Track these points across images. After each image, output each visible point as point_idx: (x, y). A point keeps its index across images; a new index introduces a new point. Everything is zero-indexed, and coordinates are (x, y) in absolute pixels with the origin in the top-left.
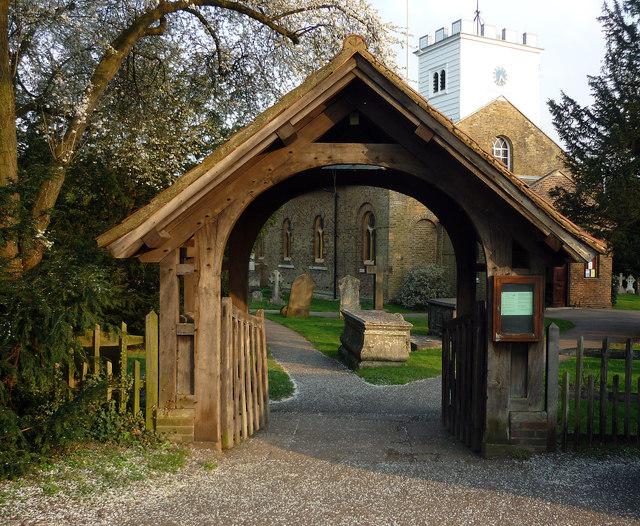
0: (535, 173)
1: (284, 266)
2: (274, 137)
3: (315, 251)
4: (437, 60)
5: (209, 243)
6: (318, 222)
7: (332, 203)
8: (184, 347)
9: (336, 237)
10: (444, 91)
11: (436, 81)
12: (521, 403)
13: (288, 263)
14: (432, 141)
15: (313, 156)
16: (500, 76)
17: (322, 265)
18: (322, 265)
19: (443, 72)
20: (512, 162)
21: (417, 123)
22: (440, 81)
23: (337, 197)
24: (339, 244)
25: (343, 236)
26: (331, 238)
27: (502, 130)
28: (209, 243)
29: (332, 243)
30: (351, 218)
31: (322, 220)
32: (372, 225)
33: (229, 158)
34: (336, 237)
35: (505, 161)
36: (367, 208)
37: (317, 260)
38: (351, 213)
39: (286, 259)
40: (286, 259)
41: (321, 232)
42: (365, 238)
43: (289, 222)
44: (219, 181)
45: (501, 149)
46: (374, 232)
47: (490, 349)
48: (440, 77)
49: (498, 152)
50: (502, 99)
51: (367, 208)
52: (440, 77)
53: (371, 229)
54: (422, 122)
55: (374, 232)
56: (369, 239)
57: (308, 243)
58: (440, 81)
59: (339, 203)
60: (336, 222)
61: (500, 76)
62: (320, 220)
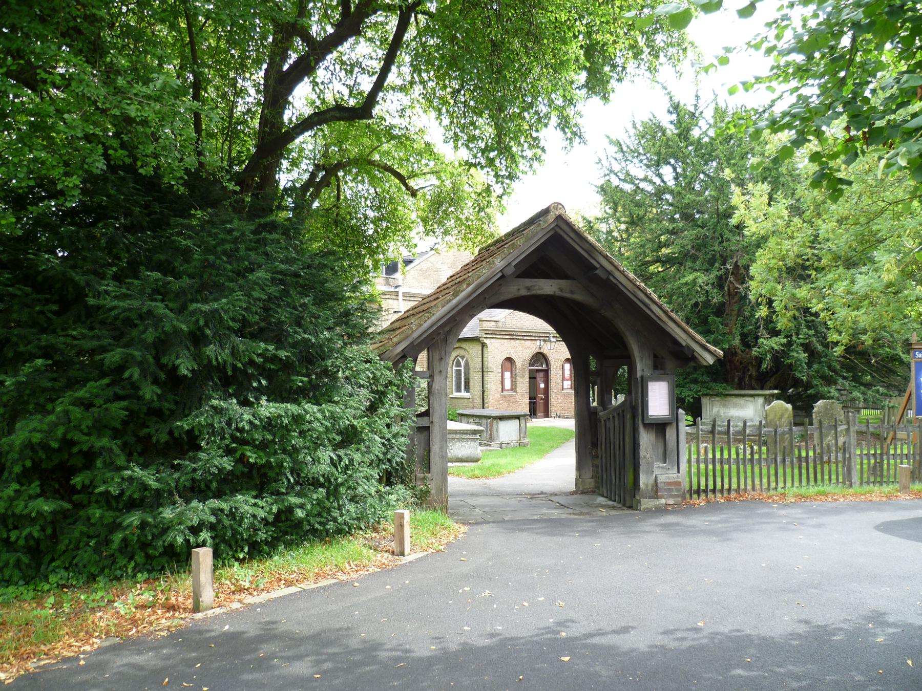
2: (500, 275)
5: (440, 354)
8: (422, 436)
12: (663, 468)
14: (608, 279)
15: (516, 288)
21: (597, 266)
28: (440, 354)
33: (469, 289)
44: (460, 307)
47: (642, 430)
54: (601, 266)
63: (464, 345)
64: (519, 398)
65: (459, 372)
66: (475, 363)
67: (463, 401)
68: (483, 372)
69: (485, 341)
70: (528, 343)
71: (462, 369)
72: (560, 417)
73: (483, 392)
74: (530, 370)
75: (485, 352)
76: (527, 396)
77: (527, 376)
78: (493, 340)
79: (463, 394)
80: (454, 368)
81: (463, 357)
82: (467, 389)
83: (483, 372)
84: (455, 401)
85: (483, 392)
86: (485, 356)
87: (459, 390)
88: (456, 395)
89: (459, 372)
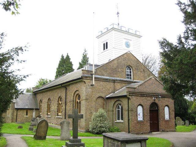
0: (141, 80)
1: (47, 116)
3: (58, 111)
4: (104, 40)
6: (60, 99)
7: (65, 90)
9: (66, 104)
10: (107, 49)
11: (104, 46)
13: (49, 115)
16: (128, 45)
17: (60, 115)
18: (60, 115)
19: (107, 43)
20: (133, 76)
22: (105, 46)
23: (66, 89)
24: (67, 107)
25: (68, 104)
26: (64, 105)
27: (129, 63)
29: (64, 107)
30: (70, 97)
31: (61, 98)
32: (79, 99)
34: (66, 104)
35: (130, 75)
36: (77, 93)
37: (59, 114)
38: (71, 95)
39: (49, 114)
40: (49, 114)
41: (60, 103)
42: (77, 104)
43: (50, 100)
45: (129, 71)
46: (80, 102)
48: (105, 45)
49: (128, 72)
50: (129, 52)
51: (77, 93)
52: (105, 45)
53: (79, 101)
55: (80, 102)
56: (78, 105)
57: (56, 107)
58: (105, 46)
59: (67, 91)
60: (66, 99)
61: (128, 45)
62: (60, 98)
63: (121, 99)
64: (145, 123)
65: (119, 111)
66: (125, 107)
67: (120, 124)
68: (128, 111)
69: (130, 97)
70: (149, 98)
71: (120, 109)
72: (164, 131)
73: (129, 120)
74: (150, 110)
75: (130, 102)
76: (149, 122)
77: (149, 113)
78: (133, 97)
79: (121, 121)
80: (117, 109)
81: (120, 104)
82: (122, 119)
83: (128, 111)
84: (117, 124)
85: (129, 120)
86: (130, 103)
87: (119, 119)
88: (118, 121)
89: (119, 111)
